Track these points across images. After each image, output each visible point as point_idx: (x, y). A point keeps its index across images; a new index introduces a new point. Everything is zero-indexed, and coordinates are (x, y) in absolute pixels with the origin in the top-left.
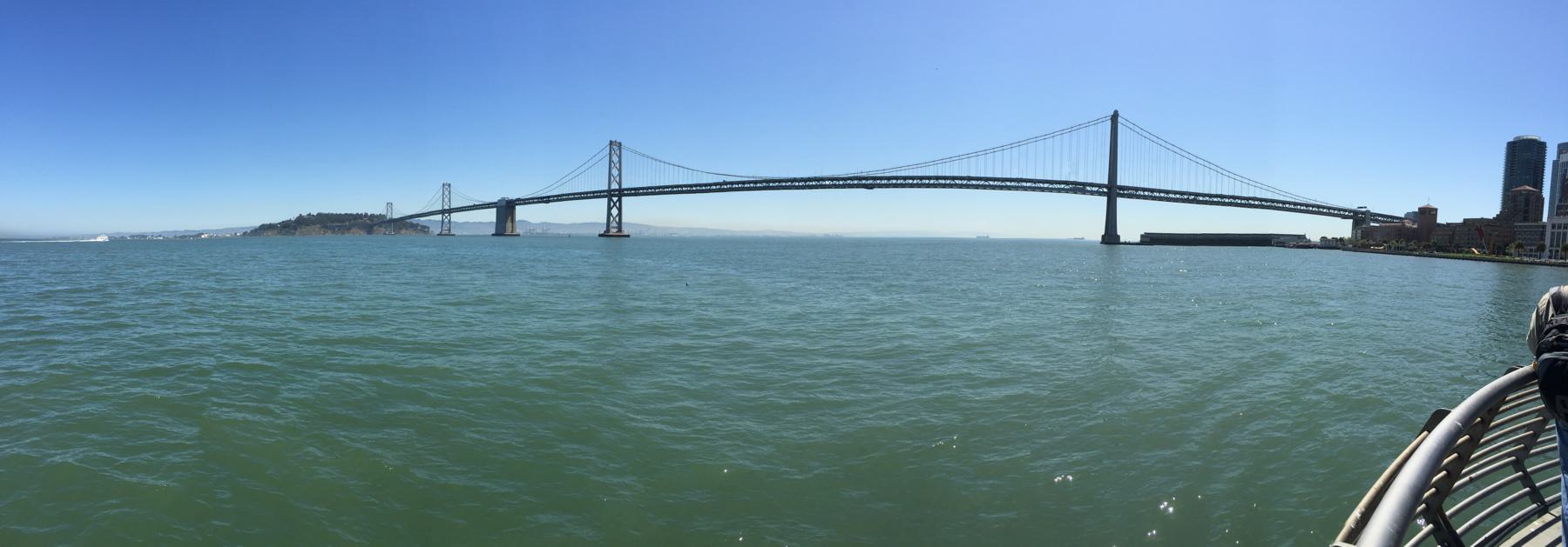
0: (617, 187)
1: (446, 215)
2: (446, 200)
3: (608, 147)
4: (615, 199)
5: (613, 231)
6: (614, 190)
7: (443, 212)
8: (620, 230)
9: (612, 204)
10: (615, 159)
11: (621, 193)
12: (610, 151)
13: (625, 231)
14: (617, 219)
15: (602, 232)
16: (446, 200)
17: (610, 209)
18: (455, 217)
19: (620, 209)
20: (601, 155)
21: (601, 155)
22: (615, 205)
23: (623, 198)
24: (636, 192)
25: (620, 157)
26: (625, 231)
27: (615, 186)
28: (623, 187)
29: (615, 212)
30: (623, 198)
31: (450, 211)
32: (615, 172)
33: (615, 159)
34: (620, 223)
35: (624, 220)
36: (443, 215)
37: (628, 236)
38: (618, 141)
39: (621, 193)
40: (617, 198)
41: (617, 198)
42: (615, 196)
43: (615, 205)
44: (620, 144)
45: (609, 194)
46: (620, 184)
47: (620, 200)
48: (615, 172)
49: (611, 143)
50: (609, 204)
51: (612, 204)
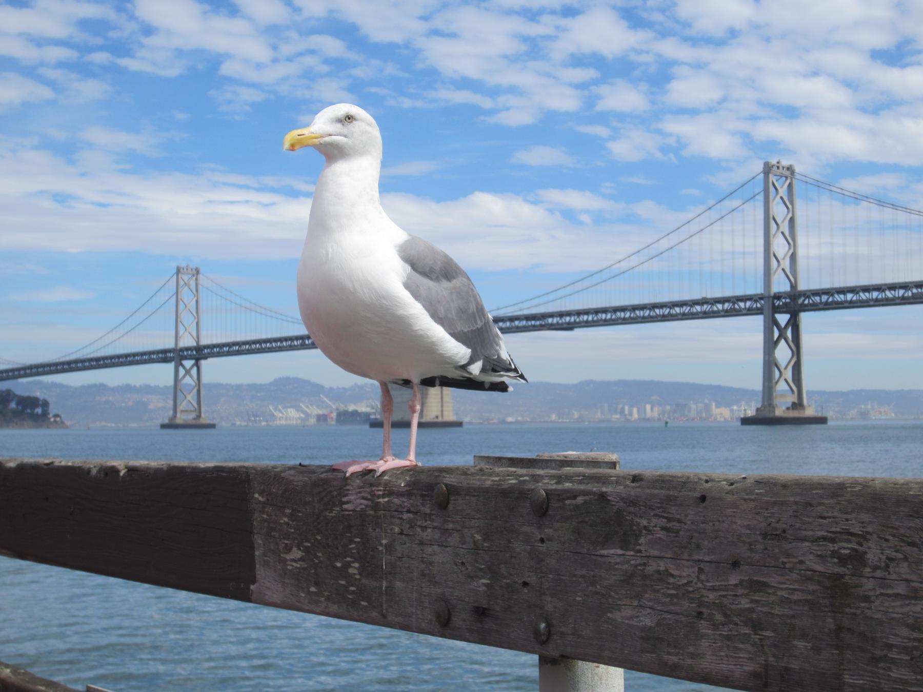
0: (785, 287)
1: (188, 363)
3: (762, 175)
8: (798, 405)
15: (751, 413)
16: (188, 319)
22: (782, 335)
28: (802, 286)
31: (200, 353)
36: (179, 364)
47: (794, 324)
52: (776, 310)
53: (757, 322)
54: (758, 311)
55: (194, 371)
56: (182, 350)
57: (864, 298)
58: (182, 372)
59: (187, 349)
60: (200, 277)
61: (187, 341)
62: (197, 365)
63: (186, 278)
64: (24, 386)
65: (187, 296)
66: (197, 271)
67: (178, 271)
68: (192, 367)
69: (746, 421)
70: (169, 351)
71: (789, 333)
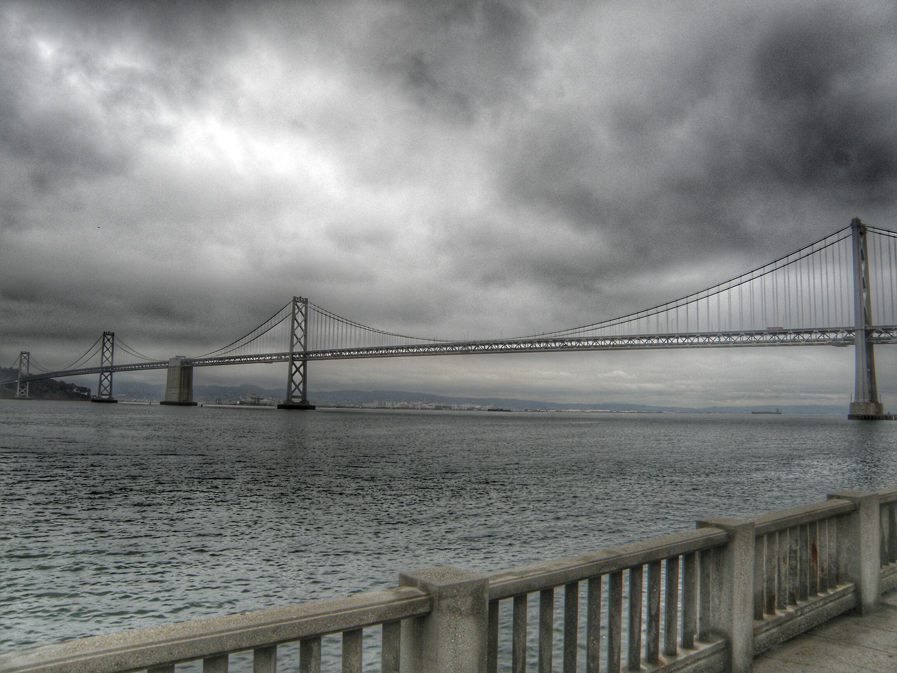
1: (106, 374)
3: (292, 303)
4: (298, 363)
6: (294, 354)
7: (102, 370)
9: (294, 369)
12: (294, 310)
13: (311, 401)
14: (301, 387)
15: (282, 403)
17: (291, 375)
18: (118, 376)
19: (304, 376)
22: (298, 369)
25: (305, 316)
28: (309, 349)
29: (298, 378)
30: (309, 363)
31: (112, 369)
34: (304, 393)
35: (309, 389)
39: (306, 357)
42: (298, 359)
43: (298, 369)
44: (306, 300)
45: (292, 358)
46: (305, 347)
47: (304, 365)
50: (291, 369)
51: (294, 369)
52: (294, 359)
54: (286, 360)
55: (109, 378)
56: (103, 368)
57: (508, 347)
58: (103, 377)
59: (107, 368)
61: (107, 364)
62: (111, 374)
64: (67, 380)
66: (113, 333)
69: (280, 407)
70: (99, 368)
71: (301, 370)
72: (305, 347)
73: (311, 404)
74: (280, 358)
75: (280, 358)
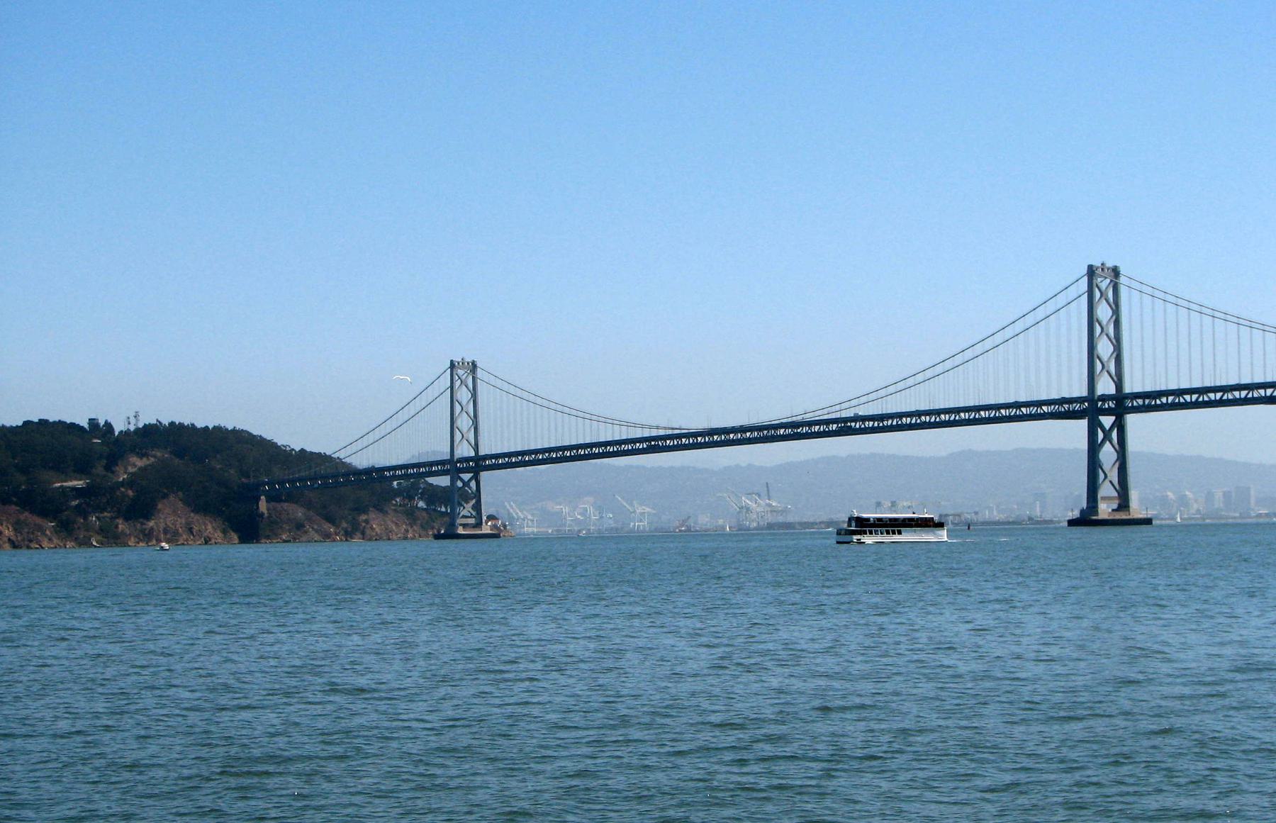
0: (1111, 390)
2: (464, 422)
3: (1086, 278)
4: (1107, 421)
5: (1105, 509)
7: (451, 466)
8: (1124, 504)
9: (1101, 435)
10: (1104, 312)
11: (1123, 404)
16: (464, 422)
20: (1072, 292)
21: (1072, 292)
22: (1107, 436)
23: (1131, 419)
24: (1153, 401)
26: (1137, 509)
27: (1105, 386)
28: (1128, 389)
29: (1108, 454)
30: (1131, 419)
31: (479, 464)
32: (1105, 348)
33: (1104, 312)
37: (1148, 521)
38: (1110, 264)
40: (1113, 418)
41: (1113, 418)
43: (1107, 436)
47: (1120, 426)
48: (1105, 348)
49: (1091, 272)
53: (1083, 423)
55: (473, 484)
60: (479, 373)
61: (464, 450)
63: (460, 372)
65: (464, 395)
67: (453, 366)
68: (470, 480)
69: (1072, 523)
71: (1114, 434)
72: (1119, 384)
73: (1142, 515)
74: (1062, 410)
75: (1062, 410)
